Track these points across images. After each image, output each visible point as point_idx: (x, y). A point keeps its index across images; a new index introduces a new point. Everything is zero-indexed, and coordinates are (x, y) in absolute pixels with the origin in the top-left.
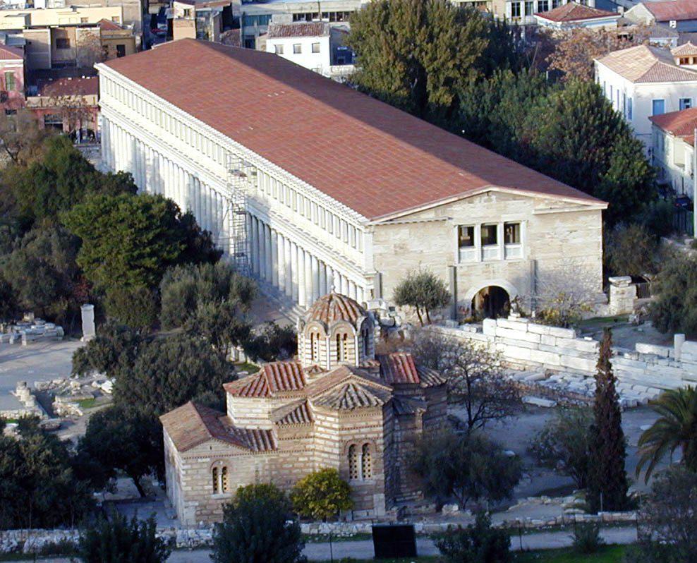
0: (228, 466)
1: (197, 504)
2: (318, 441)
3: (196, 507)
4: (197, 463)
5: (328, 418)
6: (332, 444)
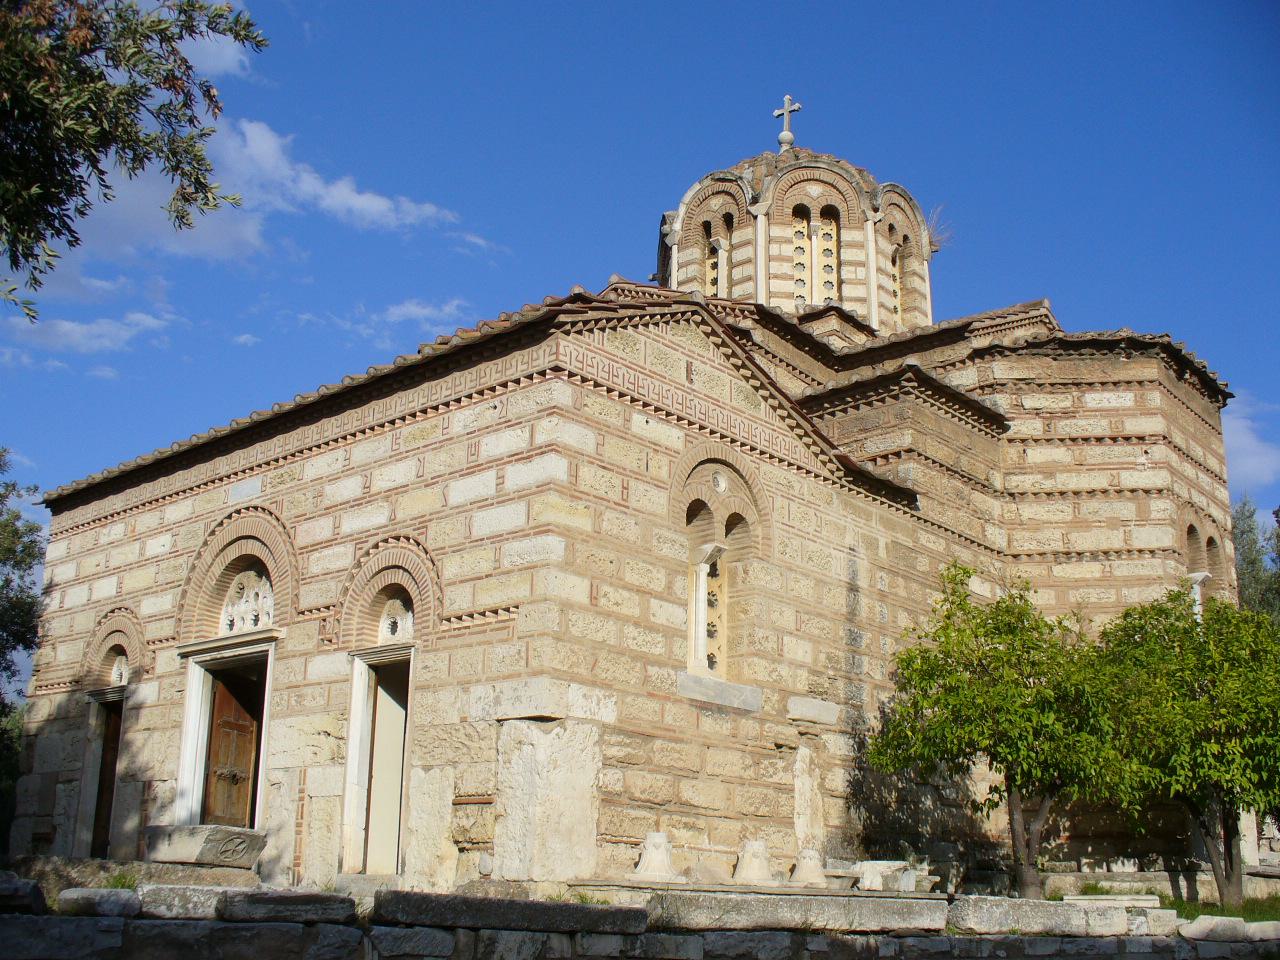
0: (750, 516)
1: (609, 714)
2: (1028, 511)
3: (605, 728)
4: (624, 434)
5: (1093, 399)
6: (1126, 509)
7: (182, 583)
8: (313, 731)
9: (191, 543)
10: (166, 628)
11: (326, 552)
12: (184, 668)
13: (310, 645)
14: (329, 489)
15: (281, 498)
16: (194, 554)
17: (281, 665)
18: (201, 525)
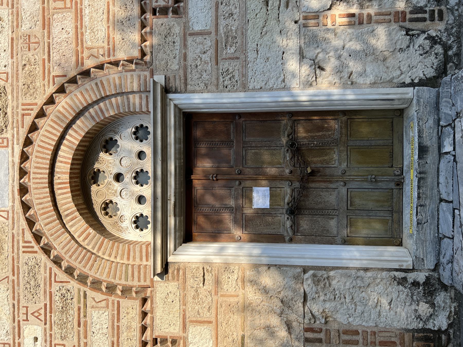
7: (83, 288)
8: (264, 10)
9: (42, 275)
10: (131, 308)
11: (86, 19)
12: (178, 270)
13: (177, 30)
14: (25, 28)
15: (20, 107)
16: (55, 269)
17: (193, 76)
18: (24, 257)
